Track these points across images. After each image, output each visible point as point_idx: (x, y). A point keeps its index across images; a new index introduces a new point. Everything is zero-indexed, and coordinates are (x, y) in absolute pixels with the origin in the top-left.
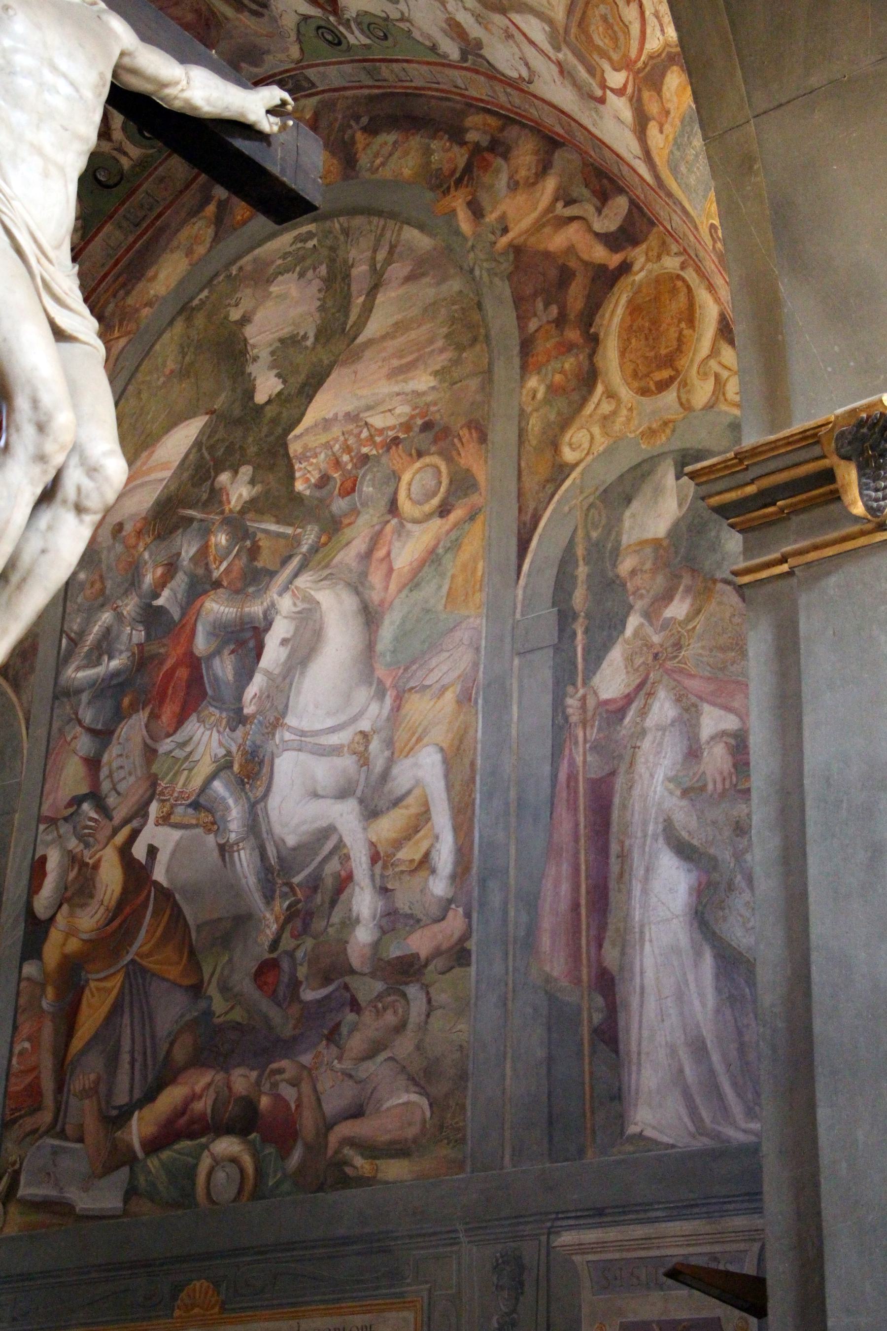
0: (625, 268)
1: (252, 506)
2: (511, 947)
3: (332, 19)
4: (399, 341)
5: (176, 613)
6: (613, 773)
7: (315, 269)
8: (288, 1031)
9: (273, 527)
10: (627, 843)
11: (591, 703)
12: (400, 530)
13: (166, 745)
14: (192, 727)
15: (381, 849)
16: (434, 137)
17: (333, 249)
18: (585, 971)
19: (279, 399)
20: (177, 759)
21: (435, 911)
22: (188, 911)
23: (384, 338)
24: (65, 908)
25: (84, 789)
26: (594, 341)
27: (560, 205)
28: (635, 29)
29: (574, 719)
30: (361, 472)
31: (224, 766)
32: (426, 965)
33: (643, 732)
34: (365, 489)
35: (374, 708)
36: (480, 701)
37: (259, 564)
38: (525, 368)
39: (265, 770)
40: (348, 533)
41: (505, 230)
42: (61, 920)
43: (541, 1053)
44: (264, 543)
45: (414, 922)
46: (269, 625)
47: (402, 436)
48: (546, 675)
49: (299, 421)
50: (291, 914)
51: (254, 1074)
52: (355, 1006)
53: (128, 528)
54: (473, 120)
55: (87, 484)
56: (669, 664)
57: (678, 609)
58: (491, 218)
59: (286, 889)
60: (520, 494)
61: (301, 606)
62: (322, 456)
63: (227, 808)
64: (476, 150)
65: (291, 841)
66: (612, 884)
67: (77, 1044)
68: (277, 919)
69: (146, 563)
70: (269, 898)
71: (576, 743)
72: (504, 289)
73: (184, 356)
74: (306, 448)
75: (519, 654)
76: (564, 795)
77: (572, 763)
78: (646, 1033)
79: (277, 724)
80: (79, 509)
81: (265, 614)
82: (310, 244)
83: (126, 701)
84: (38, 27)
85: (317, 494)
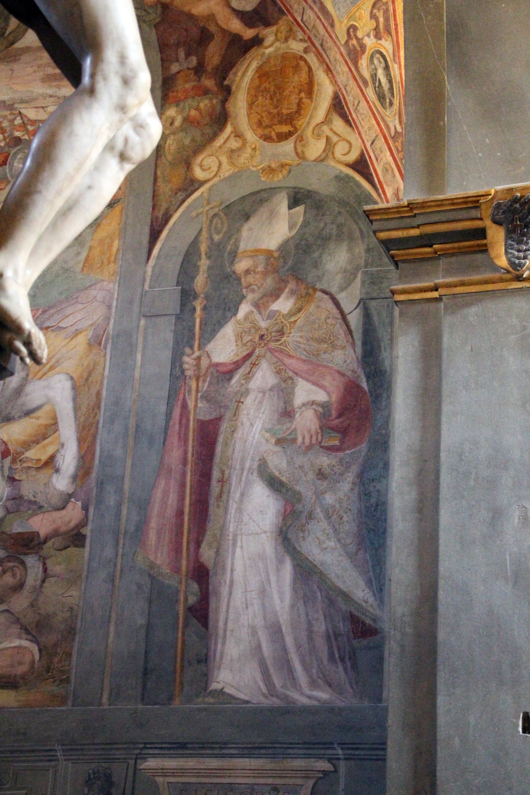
0: (257, 41)
2: (121, 536)
10: (227, 472)
11: (204, 363)
15: (10, 447)
18: (184, 563)
21: (55, 501)
29: (188, 373)
30: (13, 151)
32: (45, 542)
33: (247, 392)
34: (15, 164)
36: (109, 347)
43: (141, 621)
48: (169, 336)
56: (272, 345)
60: (155, 196)
66: (212, 501)
75: (145, 316)
76: (177, 427)
78: (231, 616)
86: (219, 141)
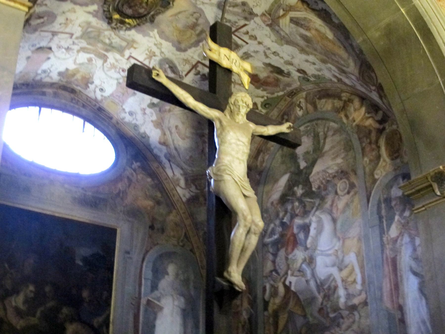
0: (384, 129)
1: (303, 195)
3: (306, 76)
4: (333, 151)
5: (288, 223)
6: (396, 256)
8: (328, 325)
9: (309, 200)
11: (389, 238)
12: (339, 199)
13: (290, 256)
16: (334, 99)
17: (314, 129)
19: (306, 168)
21: (358, 293)
24: (272, 298)
25: (272, 268)
26: (379, 147)
28: (375, 77)
29: (386, 243)
31: (304, 260)
33: (402, 245)
35: (338, 244)
38: (363, 155)
41: (354, 121)
42: (272, 301)
43: (387, 326)
44: (307, 204)
45: (354, 296)
46: (310, 224)
47: (336, 174)
48: (377, 232)
49: (311, 173)
52: (342, 318)
53: (275, 203)
54: (343, 94)
55: (256, 229)
57: (407, 214)
58: (351, 118)
60: (366, 187)
63: (306, 271)
64: (345, 102)
65: (323, 278)
70: (319, 293)
71: (387, 249)
72: (356, 136)
73: (282, 158)
74: (314, 179)
75: (370, 227)
77: (386, 254)
79: (315, 249)
80: (255, 234)
82: (309, 128)
84: (235, 133)
85: (318, 191)
86: (380, 164)
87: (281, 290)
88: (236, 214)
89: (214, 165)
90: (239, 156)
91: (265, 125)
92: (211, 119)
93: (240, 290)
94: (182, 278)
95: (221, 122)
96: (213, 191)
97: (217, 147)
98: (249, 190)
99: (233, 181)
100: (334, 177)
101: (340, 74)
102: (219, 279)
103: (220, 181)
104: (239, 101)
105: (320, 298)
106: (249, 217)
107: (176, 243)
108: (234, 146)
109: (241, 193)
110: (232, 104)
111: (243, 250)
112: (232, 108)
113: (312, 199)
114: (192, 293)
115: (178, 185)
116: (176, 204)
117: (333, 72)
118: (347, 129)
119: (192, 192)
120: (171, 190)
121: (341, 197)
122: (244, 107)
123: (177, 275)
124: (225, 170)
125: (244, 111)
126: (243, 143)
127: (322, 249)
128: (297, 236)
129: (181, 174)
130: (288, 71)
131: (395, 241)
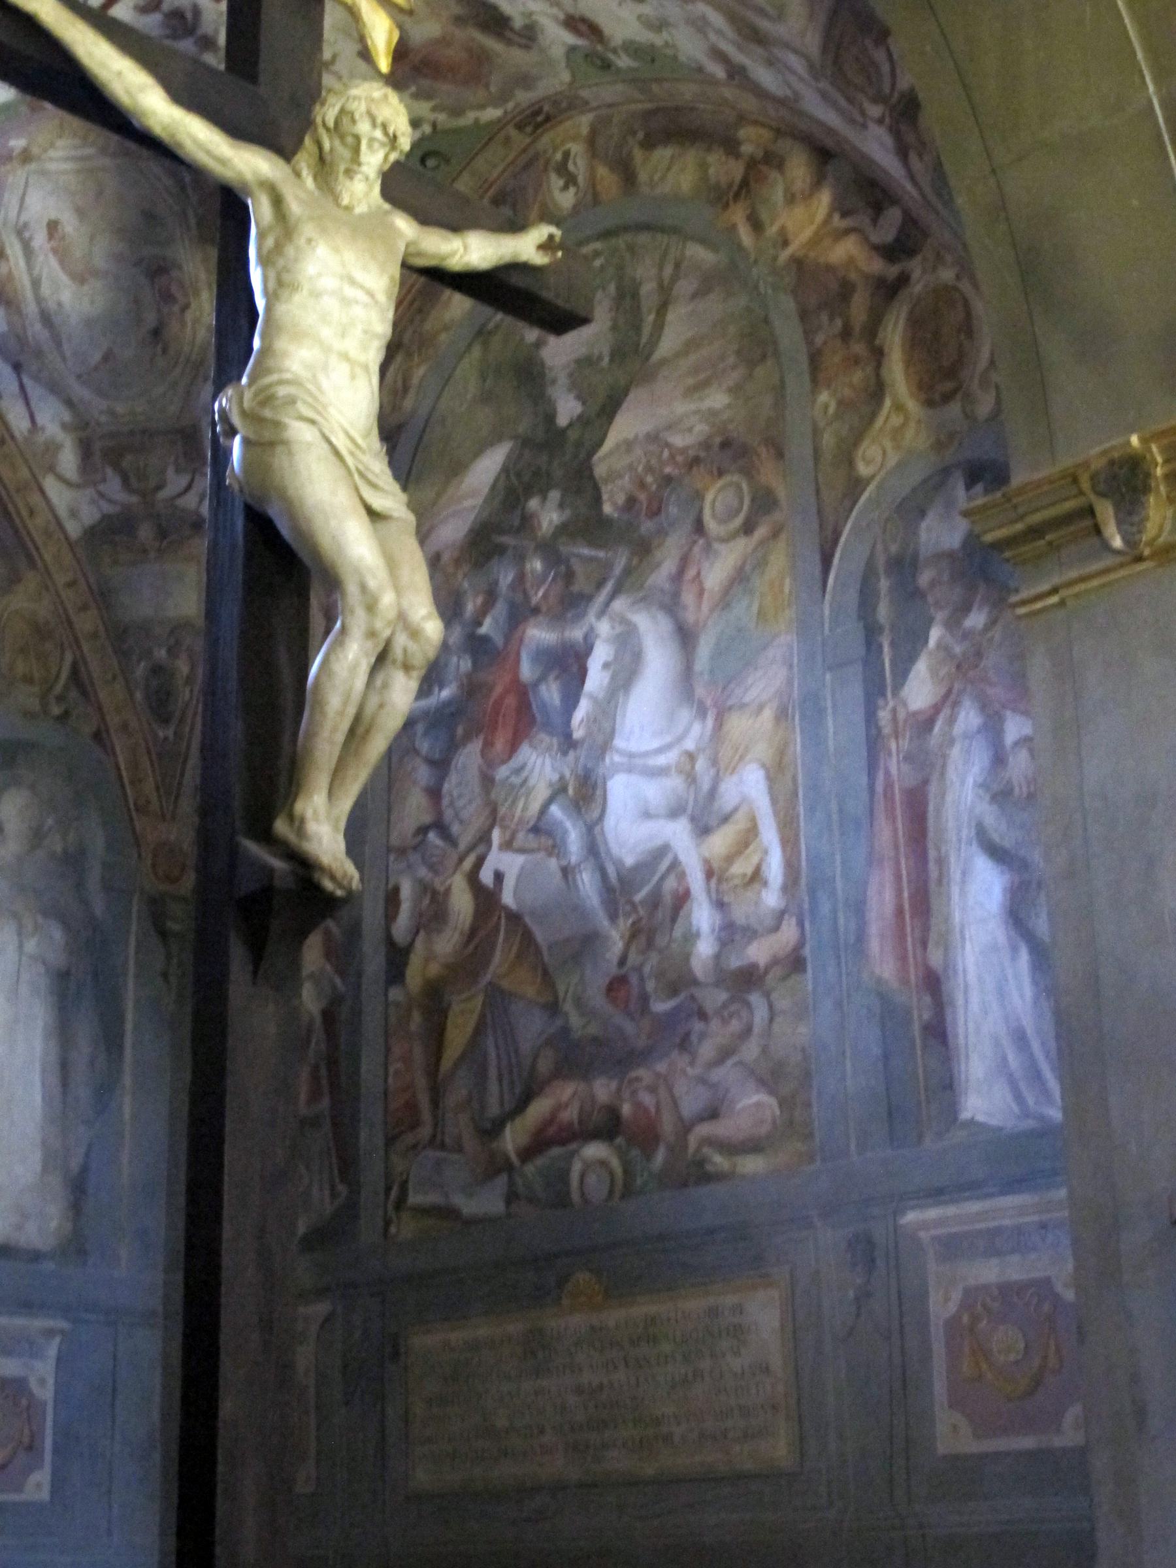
0: (903, 280)
1: (563, 530)
2: (842, 954)
3: (599, 48)
4: (693, 358)
5: (499, 640)
6: (926, 782)
7: (604, 289)
8: (641, 1043)
9: (586, 551)
10: (943, 851)
11: (901, 715)
12: (708, 548)
13: (502, 772)
14: (526, 753)
15: (715, 865)
16: (709, 150)
17: (620, 268)
18: (912, 970)
19: (582, 421)
20: (513, 787)
21: (769, 922)
22: (540, 936)
23: (678, 355)
24: (422, 933)
25: (427, 819)
26: (878, 354)
27: (836, 217)
28: (886, 68)
29: (887, 730)
31: (559, 790)
32: (766, 972)
33: (952, 742)
35: (697, 728)
36: (797, 717)
37: (575, 588)
38: (814, 381)
39: (599, 792)
40: (658, 554)
41: (786, 243)
42: (419, 944)
43: (876, 1050)
44: (578, 567)
45: (751, 933)
46: (589, 649)
47: (702, 454)
48: (857, 690)
50: (634, 933)
51: (614, 1085)
52: (703, 1016)
53: (446, 557)
55: (413, 647)
56: (971, 674)
57: (976, 619)
58: (772, 230)
59: (628, 908)
60: (820, 512)
61: (619, 629)
62: (627, 478)
63: (566, 832)
65: (629, 861)
66: (932, 886)
67: (446, 1064)
68: (622, 937)
69: (465, 592)
70: (613, 917)
71: (890, 754)
72: (789, 304)
75: (830, 669)
76: (882, 803)
77: (887, 773)
78: (971, 1025)
79: (605, 747)
80: (407, 667)
81: (586, 637)
83: (460, 731)
84: (336, 250)
86: (879, 422)
87: (462, 903)
88: (333, 582)
89: (244, 380)
90: (351, 345)
91: (455, 227)
92: (235, 184)
93: (339, 893)
94: (59, 849)
95: (277, 201)
96: (236, 487)
97: (260, 303)
98: (386, 487)
99: (325, 446)
100: (695, 461)
101: (740, 48)
102: (252, 847)
103: (272, 444)
104: (357, 116)
105: (616, 938)
106: (387, 599)
107: (34, 704)
108: (330, 303)
109: (357, 500)
110: (328, 129)
111: (357, 732)
112: (327, 145)
113: (599, 547)
114: (99, 906)
115: (52, 469)
116: (37, 549)
117: (713, 37)
118: (755, 271)
119: (110, 501)
120: (18, 491)
121: (716, 545)
122: (376, 145)
123: (37, 836)
124: (292, 401)
125: (374, 160)
126: (371, 294)
127: (634, 746)
128: (531, 694)
129: (64, 426)
130: (527, 21)
131: (925, 723)
